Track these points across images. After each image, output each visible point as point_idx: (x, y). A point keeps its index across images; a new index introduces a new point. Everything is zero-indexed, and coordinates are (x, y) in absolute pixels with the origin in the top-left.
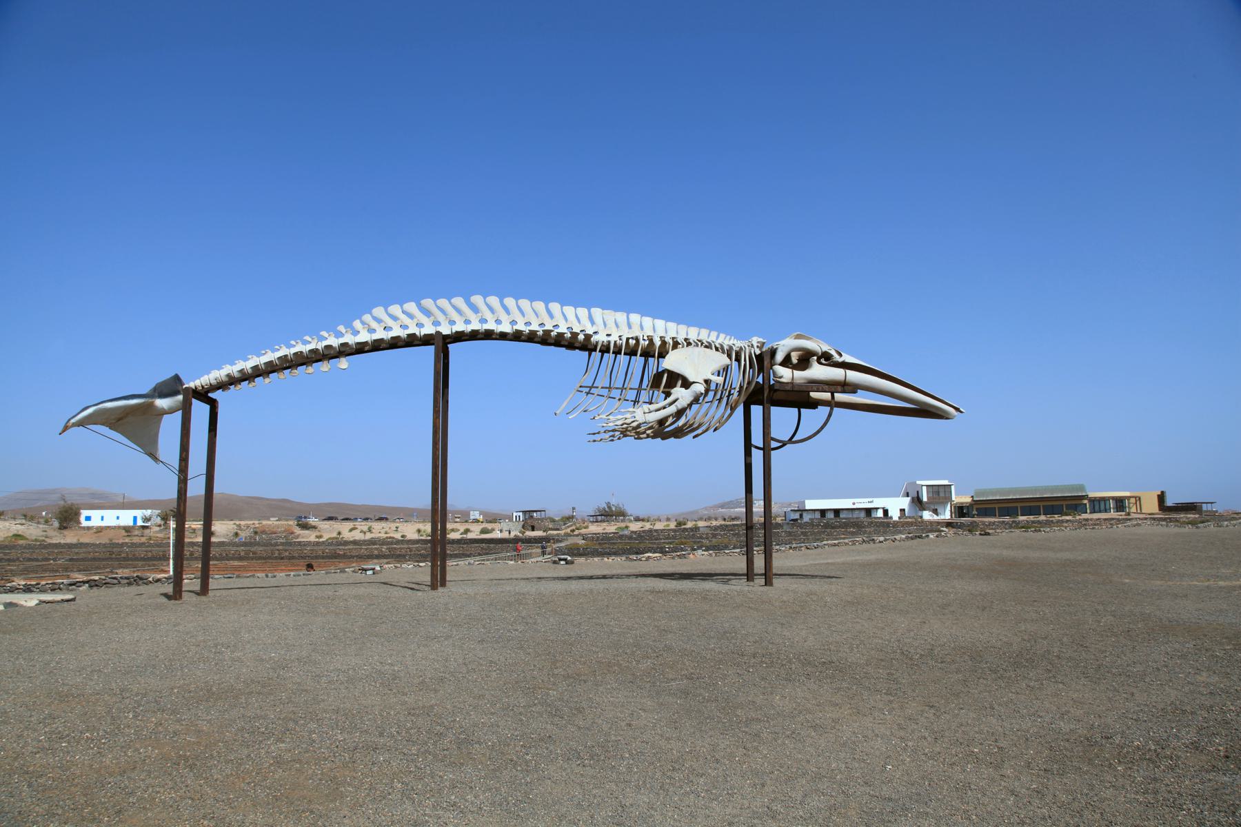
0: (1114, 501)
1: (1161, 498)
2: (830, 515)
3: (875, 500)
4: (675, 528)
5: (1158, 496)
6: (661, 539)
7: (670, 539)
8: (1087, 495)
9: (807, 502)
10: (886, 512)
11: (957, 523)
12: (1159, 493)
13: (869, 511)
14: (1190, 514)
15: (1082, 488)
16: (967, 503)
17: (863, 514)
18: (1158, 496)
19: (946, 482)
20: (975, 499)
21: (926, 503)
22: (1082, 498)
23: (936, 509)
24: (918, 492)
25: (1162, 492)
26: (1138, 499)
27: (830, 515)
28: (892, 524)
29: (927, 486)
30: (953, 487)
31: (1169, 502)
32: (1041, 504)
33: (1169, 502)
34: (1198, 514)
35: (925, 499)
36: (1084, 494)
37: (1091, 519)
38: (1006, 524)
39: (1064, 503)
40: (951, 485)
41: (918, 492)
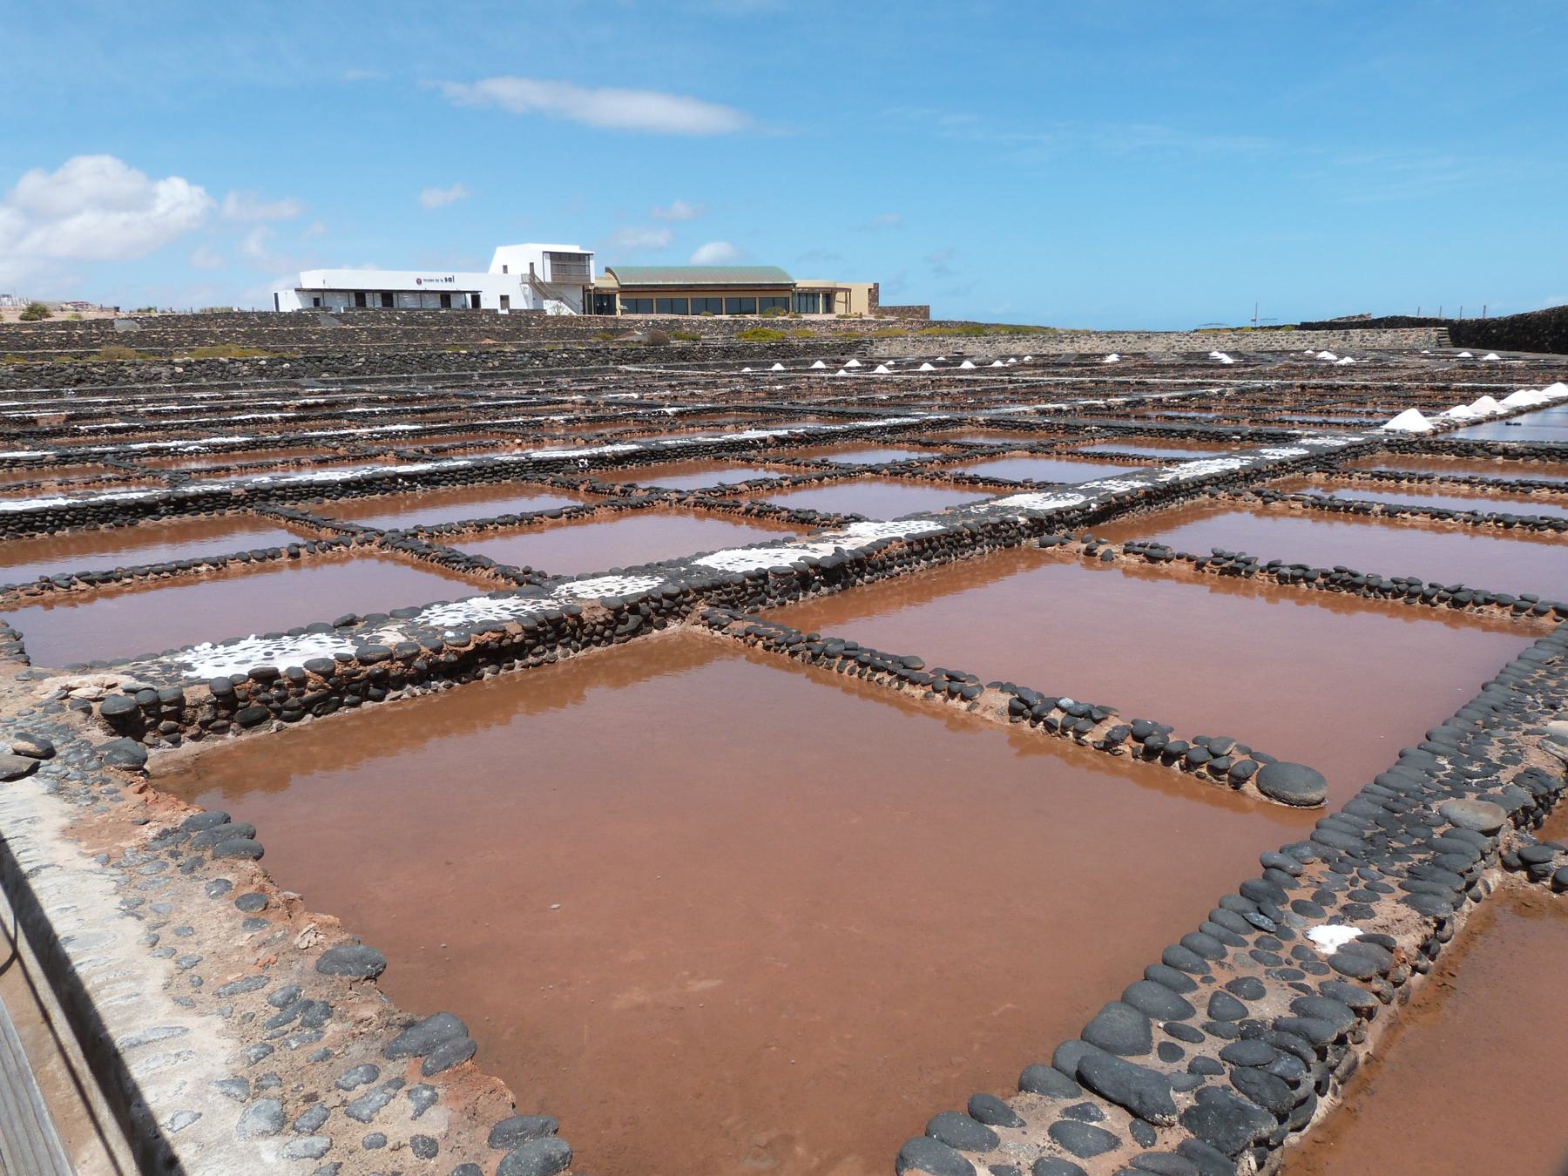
1: (874, 293)
2: (375, 304)
3: (457, 275)
4: (19, 321)
6: (49, 346)
7: (76, 345)
10: (476, 299)
11: (648, 321)
13: (446, 297)
15: (773, 270)
17: (434, 303)
25: (876, 286)
27: (375, 304)
31: (884, 301)
32: (724, 296)
33: (884, 301)
39: (758, 295)
41: (532, 264)
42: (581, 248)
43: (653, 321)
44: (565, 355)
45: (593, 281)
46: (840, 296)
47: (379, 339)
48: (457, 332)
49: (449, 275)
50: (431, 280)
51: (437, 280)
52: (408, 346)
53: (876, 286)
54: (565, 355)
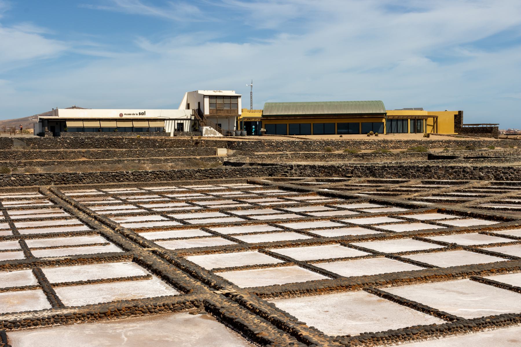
0: (413, 121)
1: (458, 117)
5: (455, 116)
8: (386, 114)
9: (60, 111)
11: (239, 142)
12: (457, 114)
14: (485, 137)
15: (379, 103)
16: (255, 118)
18: (455, 116)
19: (231, 93)
20: (264, 114)
21: (208, 117)
22: (381, 115)
23: (220, 125)
24: (199, 103)
25: (460, 113)
26: (435, 118)
28: (158, 142)
29: (210, 97)
30: (240, 100)
31: (467, 121)
33: (467, 121)
34: (493, 136)
35: (207, 112)
36: (382, 112)
37: (391, 141)
38: (295, 146)
40: (237, 97)
42: (236, 93)
43: (242, 142)
44: (13, 178)
45: (240, 113)
46: (430, 121)
47: (6, 158)
48: (61, 153)
49: (142, 111)
50: (129, 114)
51: (133, 114)
52: (20, 163)
53: (460, 113)
54: (13, 178)
